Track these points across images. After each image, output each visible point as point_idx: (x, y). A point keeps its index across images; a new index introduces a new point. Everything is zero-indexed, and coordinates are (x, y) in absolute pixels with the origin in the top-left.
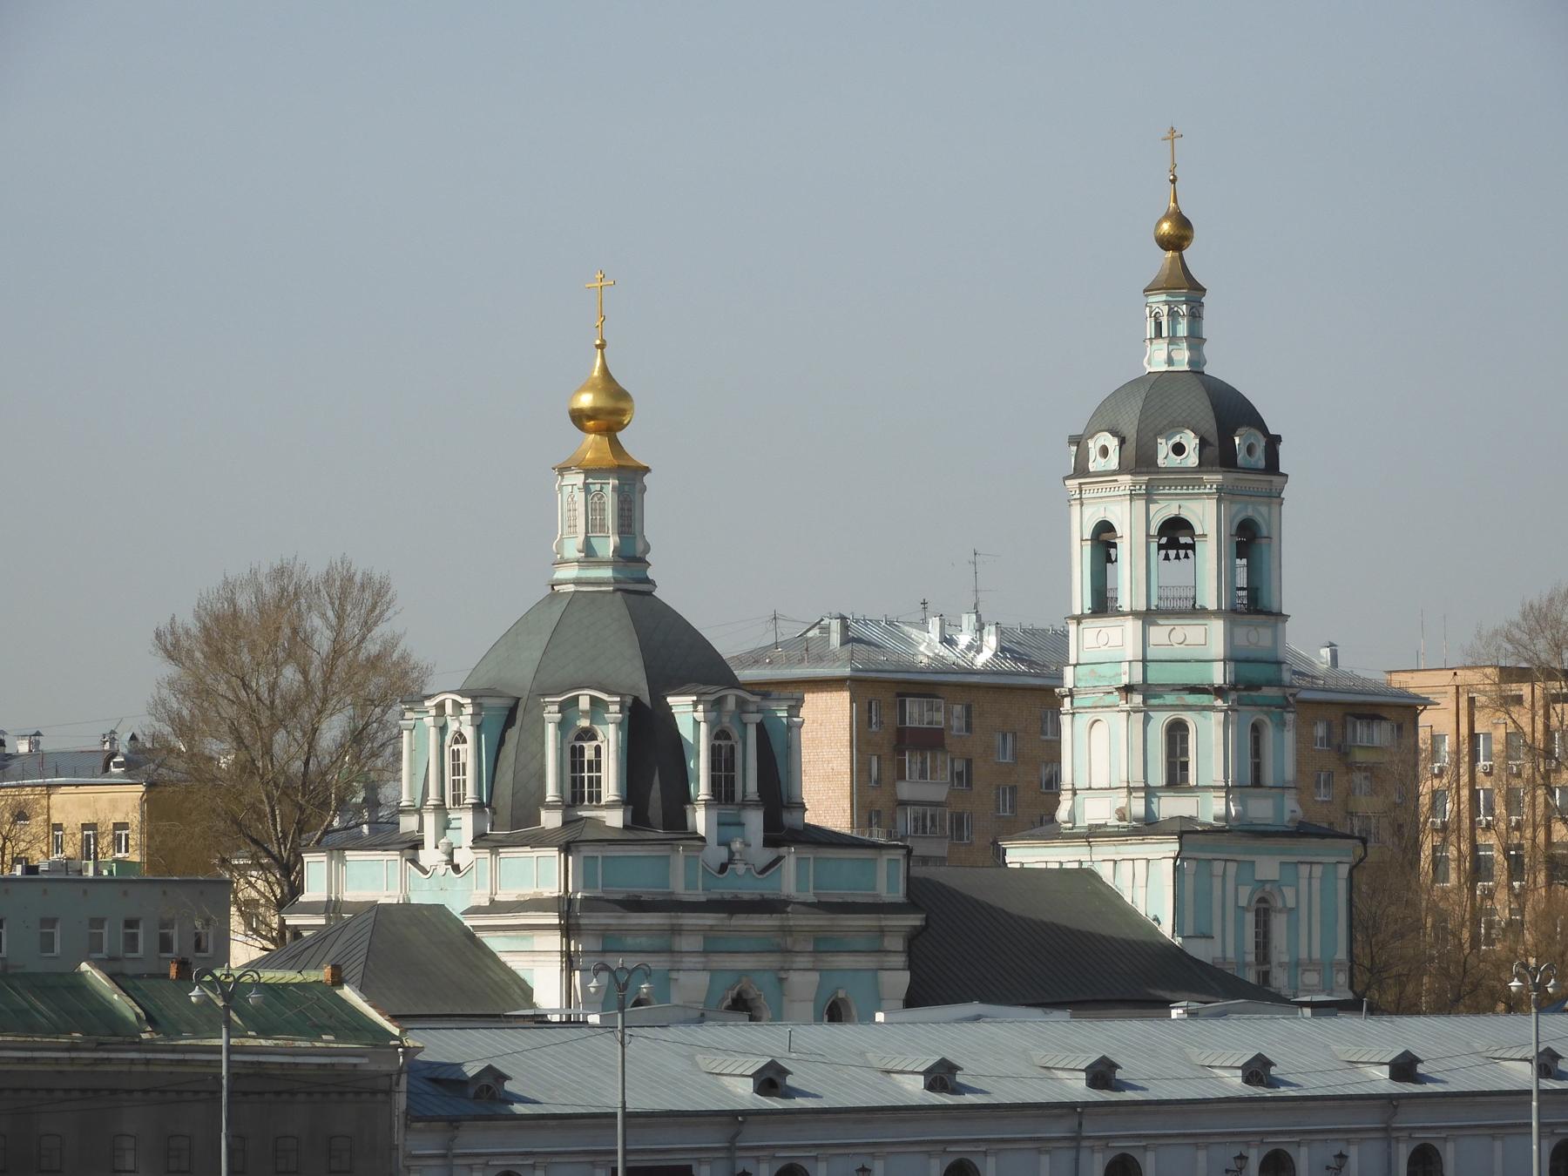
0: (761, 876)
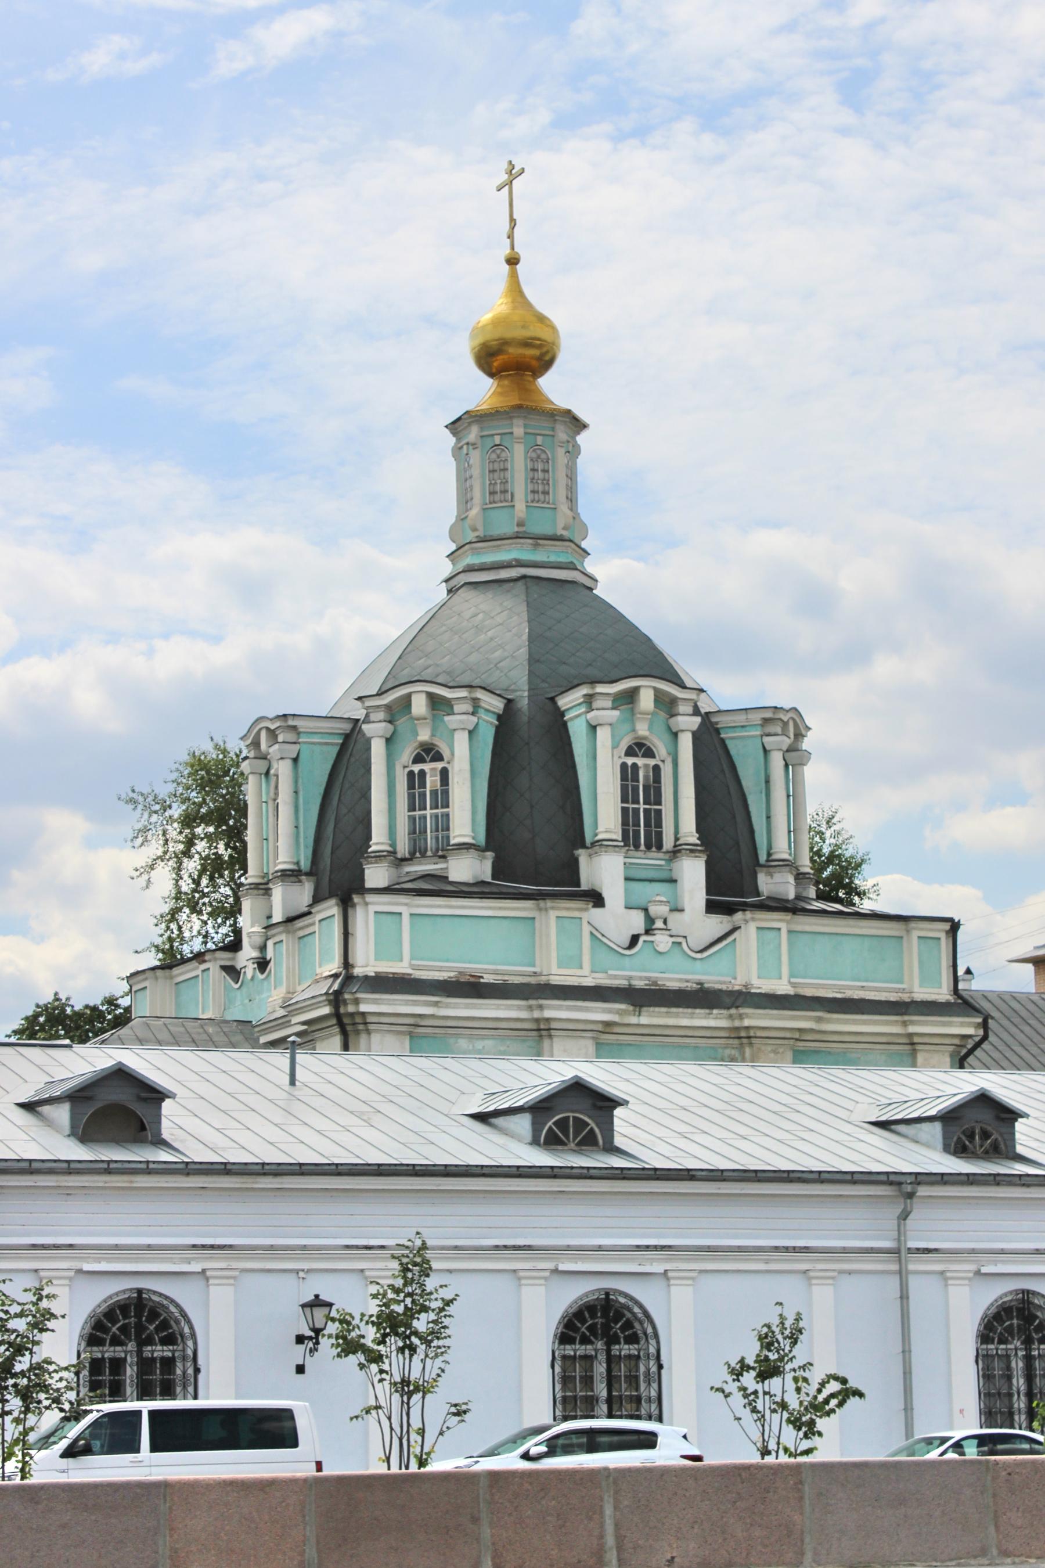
0: (699, 956)
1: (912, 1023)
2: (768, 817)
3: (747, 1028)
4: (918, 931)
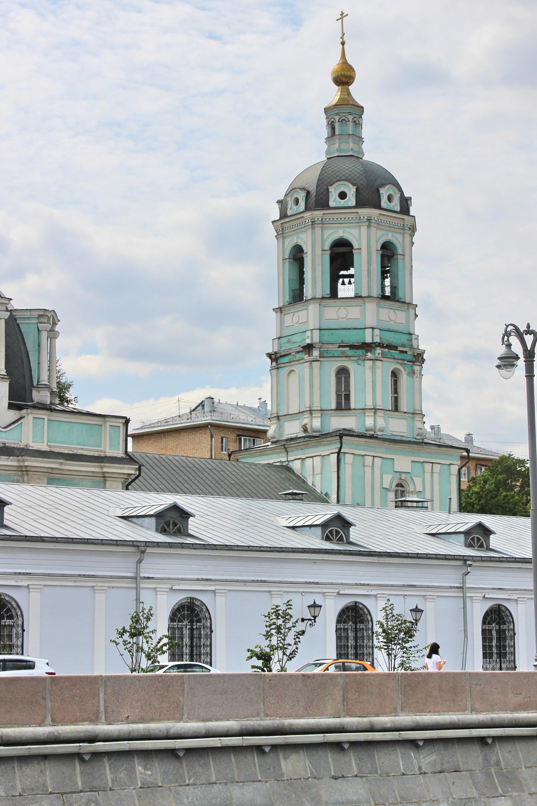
0: (4, 430)
1: (105, 467)
2: (39, 363)
3: (26, 466)
4: (110, 422)
